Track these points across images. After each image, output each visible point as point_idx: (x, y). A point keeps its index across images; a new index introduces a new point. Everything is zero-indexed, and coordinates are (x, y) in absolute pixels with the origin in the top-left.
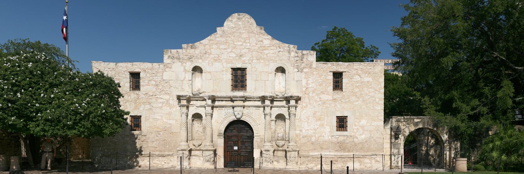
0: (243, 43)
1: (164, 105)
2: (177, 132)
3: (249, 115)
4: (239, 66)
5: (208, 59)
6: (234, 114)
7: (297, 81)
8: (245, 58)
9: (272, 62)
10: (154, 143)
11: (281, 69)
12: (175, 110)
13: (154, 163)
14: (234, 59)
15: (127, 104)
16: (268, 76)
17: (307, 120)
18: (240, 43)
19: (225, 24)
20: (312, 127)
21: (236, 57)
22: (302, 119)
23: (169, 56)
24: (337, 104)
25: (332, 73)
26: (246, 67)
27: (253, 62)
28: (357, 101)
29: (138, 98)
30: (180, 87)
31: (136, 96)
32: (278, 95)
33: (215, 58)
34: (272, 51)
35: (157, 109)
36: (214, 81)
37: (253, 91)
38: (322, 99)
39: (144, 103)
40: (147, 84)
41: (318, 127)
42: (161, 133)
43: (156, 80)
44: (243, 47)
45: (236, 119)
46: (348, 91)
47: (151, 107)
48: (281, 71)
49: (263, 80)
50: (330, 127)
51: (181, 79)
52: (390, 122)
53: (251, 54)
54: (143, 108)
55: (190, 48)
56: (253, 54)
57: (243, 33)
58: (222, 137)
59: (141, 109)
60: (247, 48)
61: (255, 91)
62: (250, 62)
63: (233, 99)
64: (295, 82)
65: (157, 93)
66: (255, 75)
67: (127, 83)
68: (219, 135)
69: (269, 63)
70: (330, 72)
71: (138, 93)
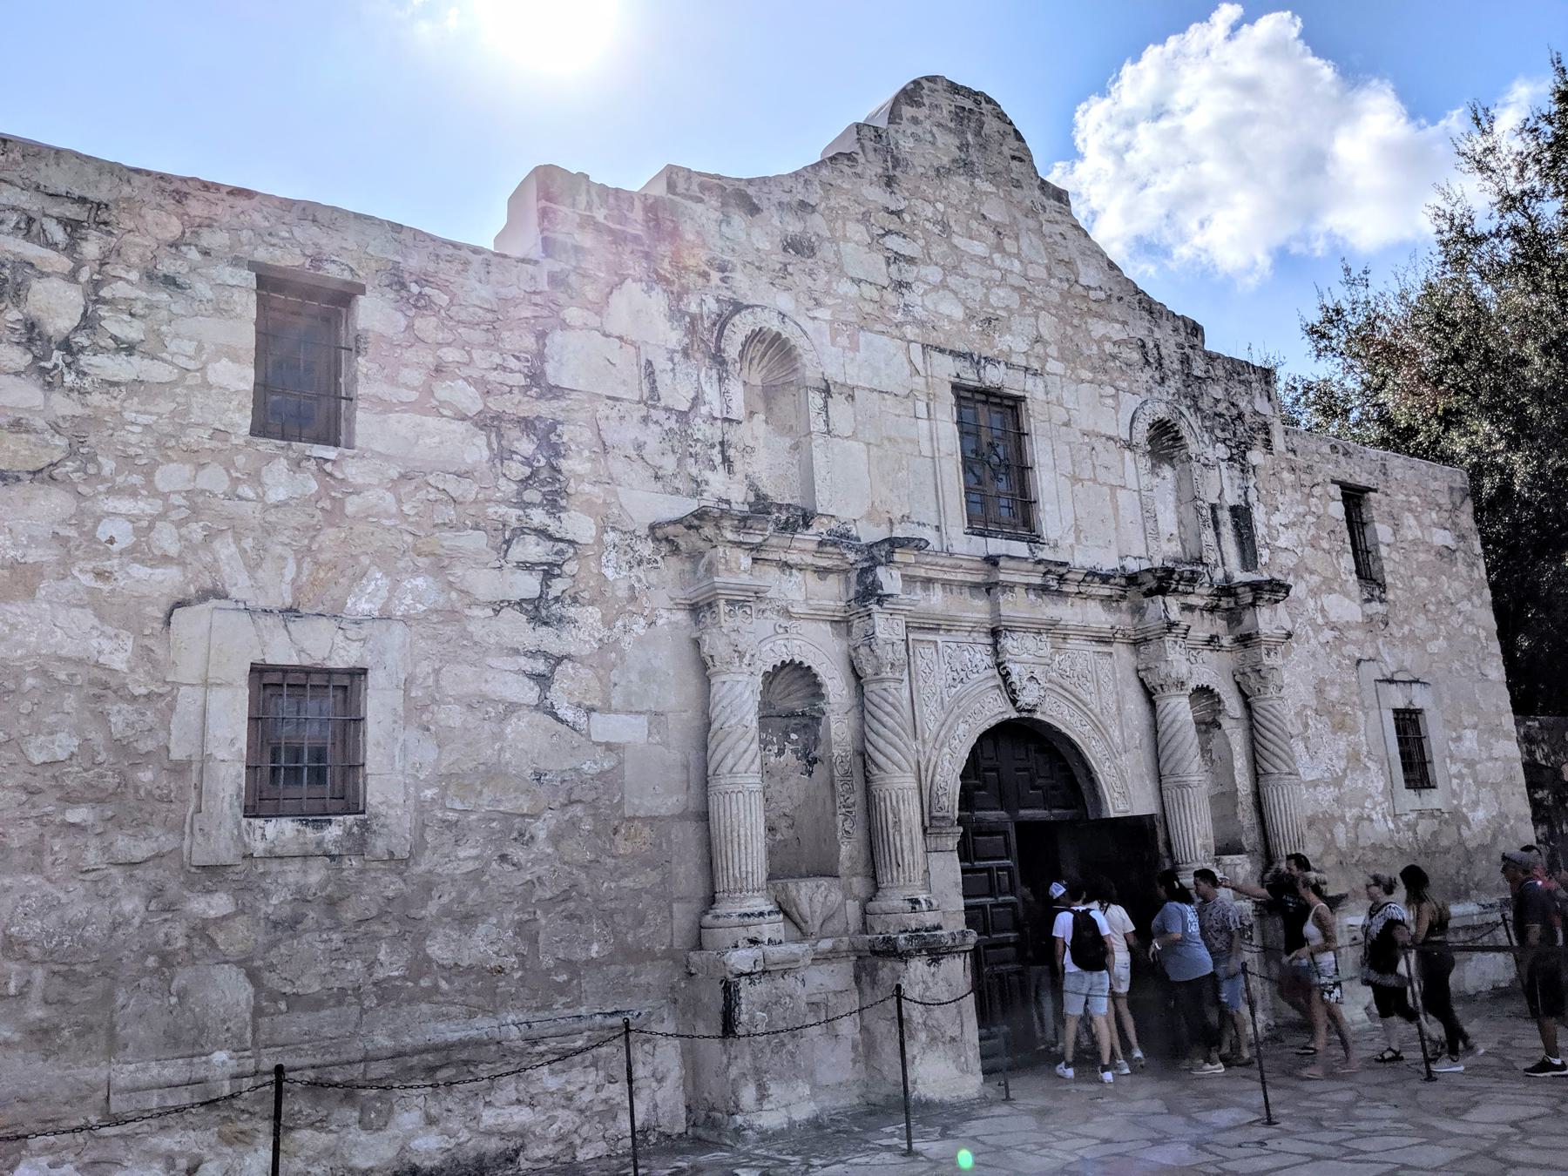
0: (991, 254)
1: (558, 586)
2: (663, 811)
3: (1072, 688)
4: (994, 376)
5: (829, 301)
6: (999, 681)
7: (1234, 510)
8: (1013, 342)
9: (1125, 385)
10: (482, 929)
12: (642, 632)
13: (489, 1133)
14: (959, 331)
15: (225, 549)
16: (1123, 458)
18: (979, 248)
20: (1323, 766)
21: (968, 326)
24: (1380, 641)
25: (1336, 491)
26: (1022, 394)
28: (1435, 637)
29: (335, 515)
30: (669, 464)
31: (314, 486)
33: (868, 308)
34: (1116, 332)
35: (508, 613)
36: (874, 450)
37: (1071, 540)
38: (1333, 617)
39: (383, 558)
40: (414, 396)
41: (1343, 764)
42: (540, 830)
43: (494, 376)
44: (997, 275)
45: (1015, 715)
46: (1400, 586)
47: (454, 595)
49: (1105, 484)
50: (1383, 764)
51: (670, 403)
53: (1033, 319)
54: (379, 603)
55: (715, 202)
56: (1041, 323)
57: (986, 193)
58: (952, 843)
59: (362, 604)
60: (1015, 288)
61: (1077, 538)
62: (1036, 365)
63: (1002, 577)
65: (502, 481)
67: (235, 359)
68: (931, 826)
70: (1333, 482)
71: (334, 462)
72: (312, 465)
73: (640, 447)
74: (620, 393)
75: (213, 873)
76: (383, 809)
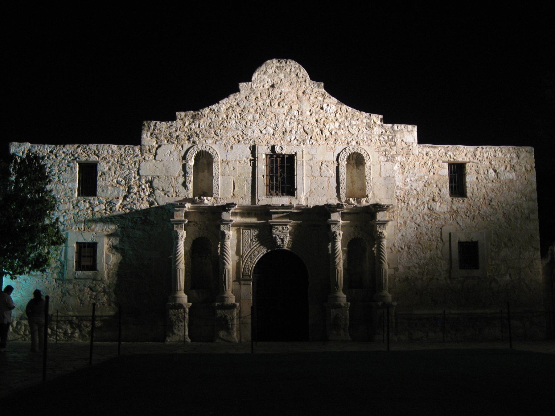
11: (355, 156)
17: (406, 249)
19: (253, 78)
22: (397, 247)
23: (152, 134)
25: (446, 165)
27: (305, 143)
31: (88, 205)
32: (353, 204)
37: (308, 196)
48: (354, 162)
52: (549, 252)
64: (383, 181)
66: (309, 167)
69: (335, 147)
70: (443, 162)
72: (88, 201)
73: (162, 187)
74: (158, 174)
75: (70, 281)
76: (100, 270)
